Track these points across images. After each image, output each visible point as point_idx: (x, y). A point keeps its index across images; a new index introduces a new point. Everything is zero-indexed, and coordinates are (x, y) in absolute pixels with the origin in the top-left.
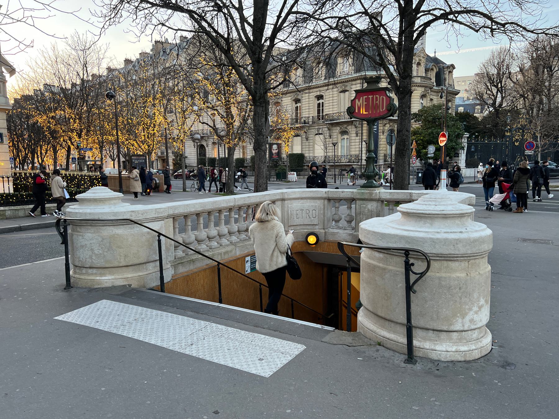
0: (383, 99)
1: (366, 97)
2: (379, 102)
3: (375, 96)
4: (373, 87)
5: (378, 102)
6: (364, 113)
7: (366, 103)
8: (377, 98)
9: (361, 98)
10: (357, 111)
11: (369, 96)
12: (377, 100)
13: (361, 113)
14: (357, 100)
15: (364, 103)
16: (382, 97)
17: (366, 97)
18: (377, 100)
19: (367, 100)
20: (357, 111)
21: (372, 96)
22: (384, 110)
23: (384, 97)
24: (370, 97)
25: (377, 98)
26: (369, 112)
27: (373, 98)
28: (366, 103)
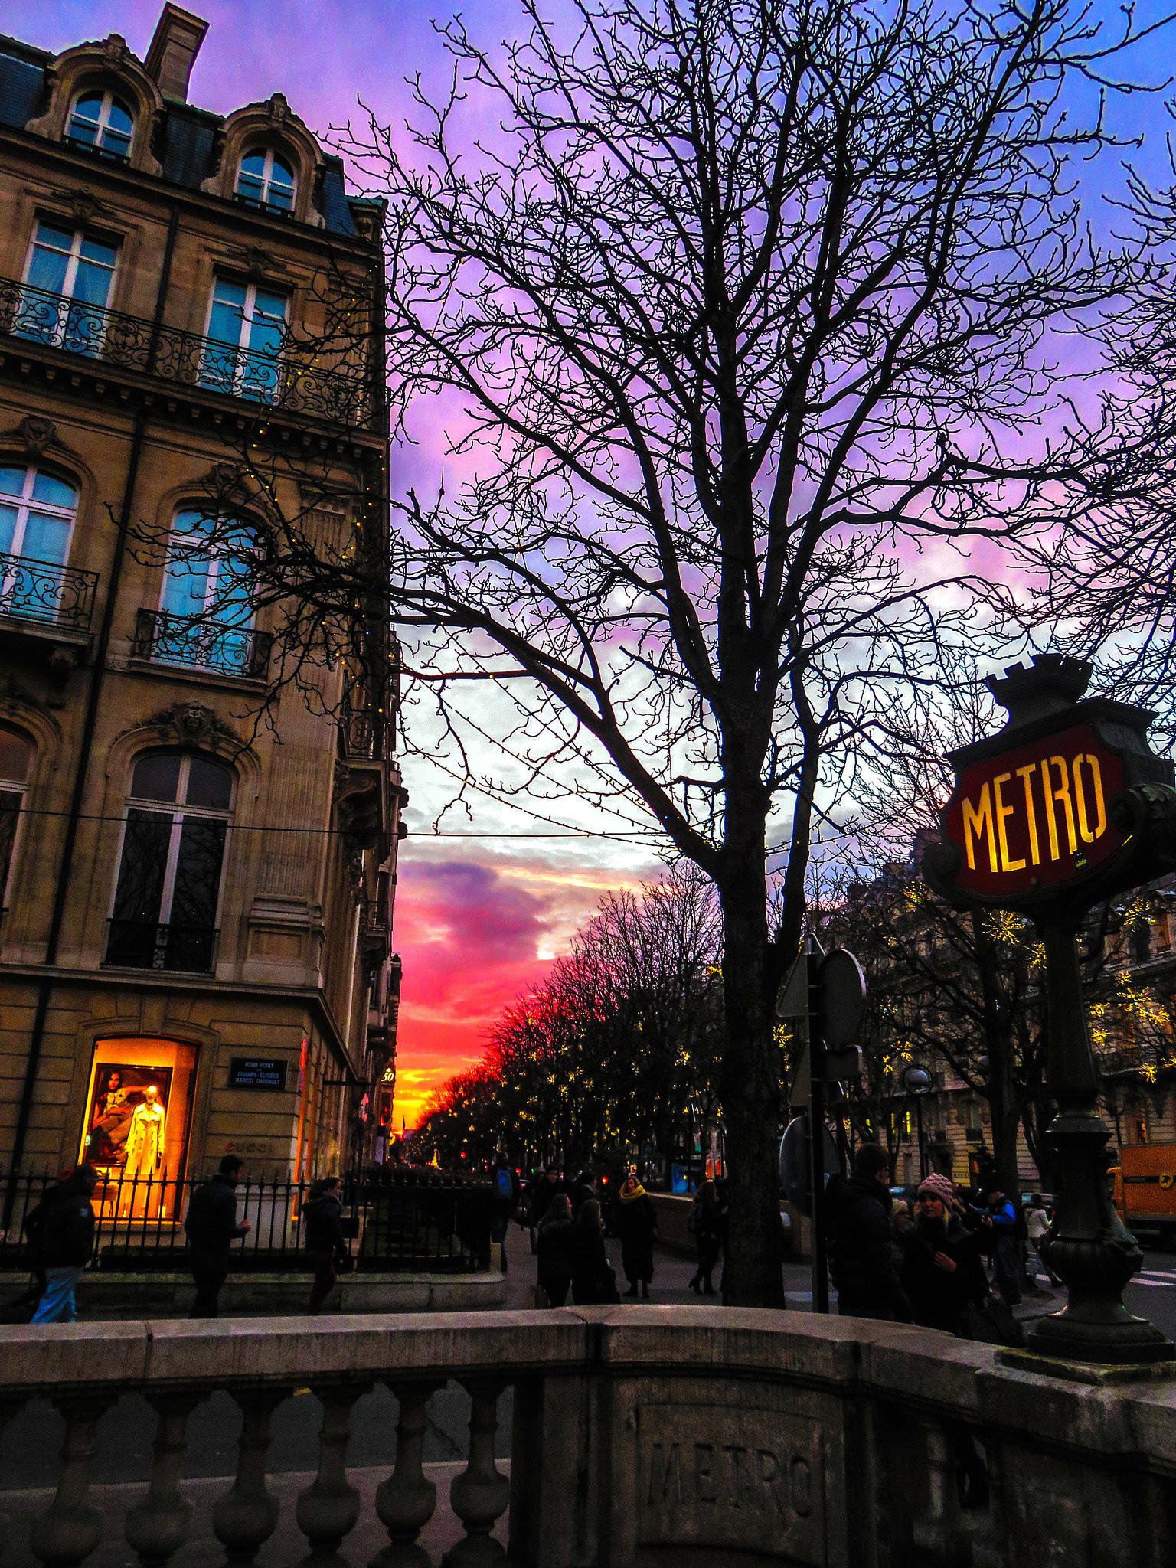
0: (1086, 769)
1: (1007, 777)
3: (1044, 764)
5: (1058, 796)
6: (1008, 866)
7: (1010, 810)
8: (1055, 771)
9: (985, 789)
10: (972, 866)
11: (1020, 772)
12: (1056, 786)
13: (994, 868)
14: (967, 805)
15: (1003, 812)
16: (1079, 759)
17: (1007, 777)
18: (1056, 786)
20: (972, 866)
21: (1033, 767)
22: (1100, 831)
23: (1092, 760)
24: (1025, 772)
25: (1055, 771)
28: (1010, 810)
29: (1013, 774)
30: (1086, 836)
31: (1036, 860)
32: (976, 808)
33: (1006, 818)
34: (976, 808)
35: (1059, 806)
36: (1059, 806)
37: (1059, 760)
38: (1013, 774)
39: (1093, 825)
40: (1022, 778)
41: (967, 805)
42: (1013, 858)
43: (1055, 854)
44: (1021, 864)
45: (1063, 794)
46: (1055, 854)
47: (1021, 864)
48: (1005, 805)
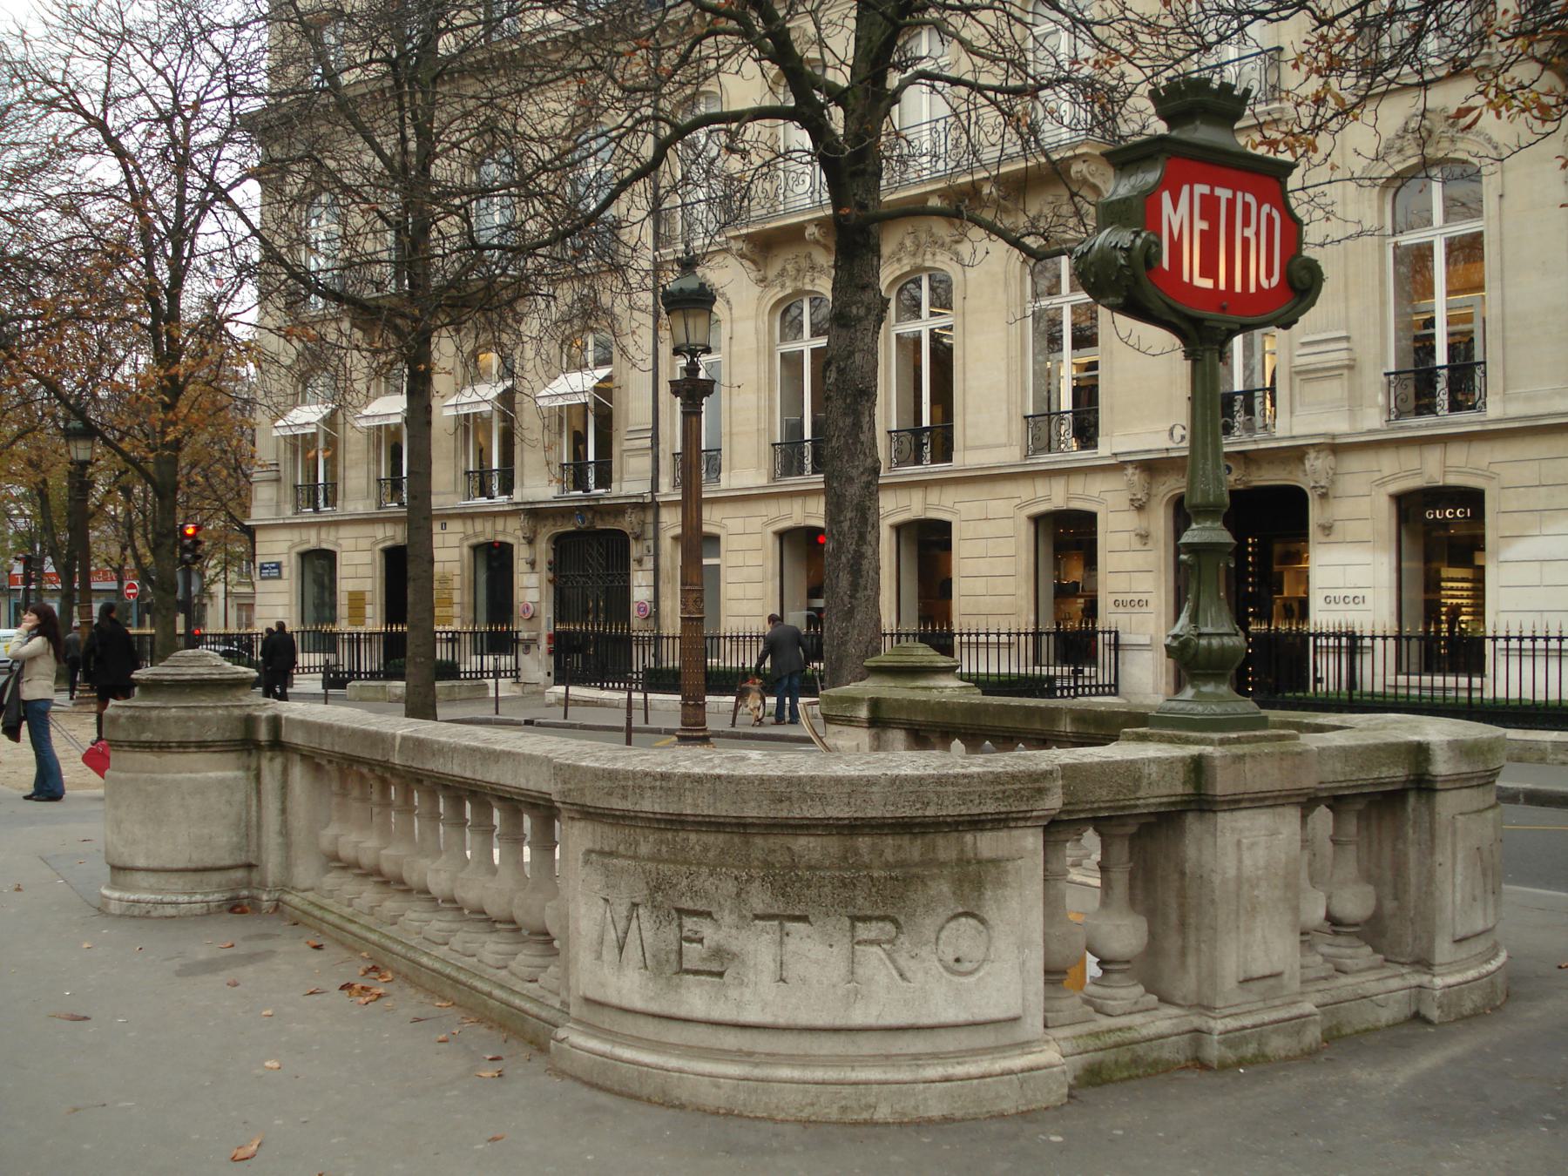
1: (1205, 189)
2: (1257, 234)
3: (1239, 195)
4: (1203, 133)
7: (1205, 226)
8: (1246, 206)
9: (1186, 189)
10: (1166, 265)
11: (1219, 191)
12: (1246, 223)
13: (1186, 278)
14: (1166, 196)
15: (1201, 225)
16: (1266, 208)
18: (1246, 223)
19: (1209, 207)
20: (1166, 265)
22: (1275, 280)
23: (1276, 214)
24: (1224, 194)
25: (1246, 206)
26: (1216, 283)
27: (1231, 203)
28: (1205, 226)
29: (1212, 190)
30: (1265, 283)
31: (1222, 286)
32: (1175, 207)
33: (1202, 232)
34: (1175, 207)
35: (1246, 241)
36: (1246, 241)
37: (1250, 198)
38: (1212, 190)
39: (1269, 275)
40: (1218, 198)
41: (1166, 196)
42: (1202, 275)
43: (1238, 288)
44: (1207, 283)
45: (1250, 232)
46: (1238, 288)
47: (1207, 283)
48: (1202, 217)
